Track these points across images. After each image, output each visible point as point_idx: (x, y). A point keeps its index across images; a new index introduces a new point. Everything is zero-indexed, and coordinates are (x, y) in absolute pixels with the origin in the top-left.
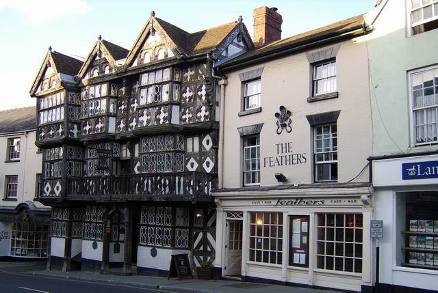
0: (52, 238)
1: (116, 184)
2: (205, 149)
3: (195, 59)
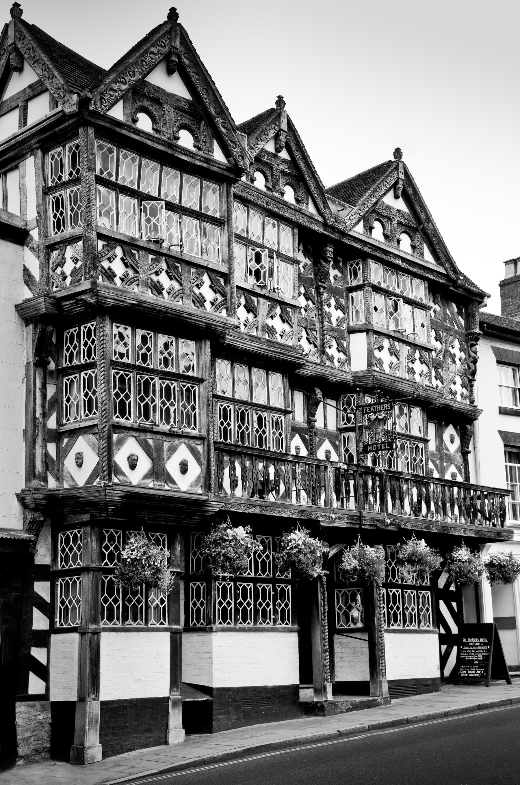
0: (103, 635)
1: (348, 485)
2: (447, 450)
3: (461, 291)
